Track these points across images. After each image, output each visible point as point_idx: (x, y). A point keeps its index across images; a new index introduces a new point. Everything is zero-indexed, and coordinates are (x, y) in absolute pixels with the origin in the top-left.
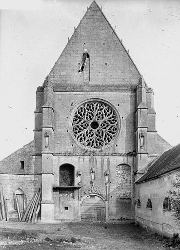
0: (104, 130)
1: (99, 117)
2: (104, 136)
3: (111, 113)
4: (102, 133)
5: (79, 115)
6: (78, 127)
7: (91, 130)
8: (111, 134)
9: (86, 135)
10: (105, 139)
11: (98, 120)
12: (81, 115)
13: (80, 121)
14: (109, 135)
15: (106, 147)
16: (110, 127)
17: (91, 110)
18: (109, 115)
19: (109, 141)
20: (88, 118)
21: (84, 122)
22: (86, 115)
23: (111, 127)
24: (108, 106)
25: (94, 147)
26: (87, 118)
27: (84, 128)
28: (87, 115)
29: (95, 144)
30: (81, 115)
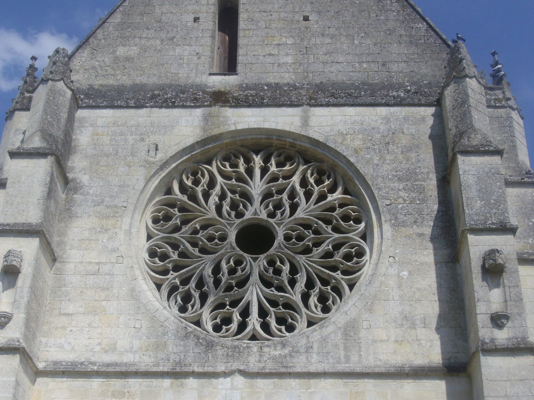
0: (301, 259)
1: (278, 206)
2: (301, 286)
3: (332, 190)
4: (294, 270)
5: (185, 198)
6: (175, 246)
7: (239, 262)
8: (338, 275)
9: (210, 281)
10: (305, 297)
11: (272, 215)
12: (193, 198)
13: (185, 222)
14: (325, 282)
15: (316, 333)
16: (326, 246)
17: (240, 179)
18: (322, 197)
19: (326, 310)
20: (226, 207)
21: (204, 227)
22: (214, 199)
23: (337, 247)
24: (321, 161)
25: (254, 338)
26: (219, 208)
27: (204, 251)
28: (222, 197)
29: (254, 320)
30: (193, 198)
